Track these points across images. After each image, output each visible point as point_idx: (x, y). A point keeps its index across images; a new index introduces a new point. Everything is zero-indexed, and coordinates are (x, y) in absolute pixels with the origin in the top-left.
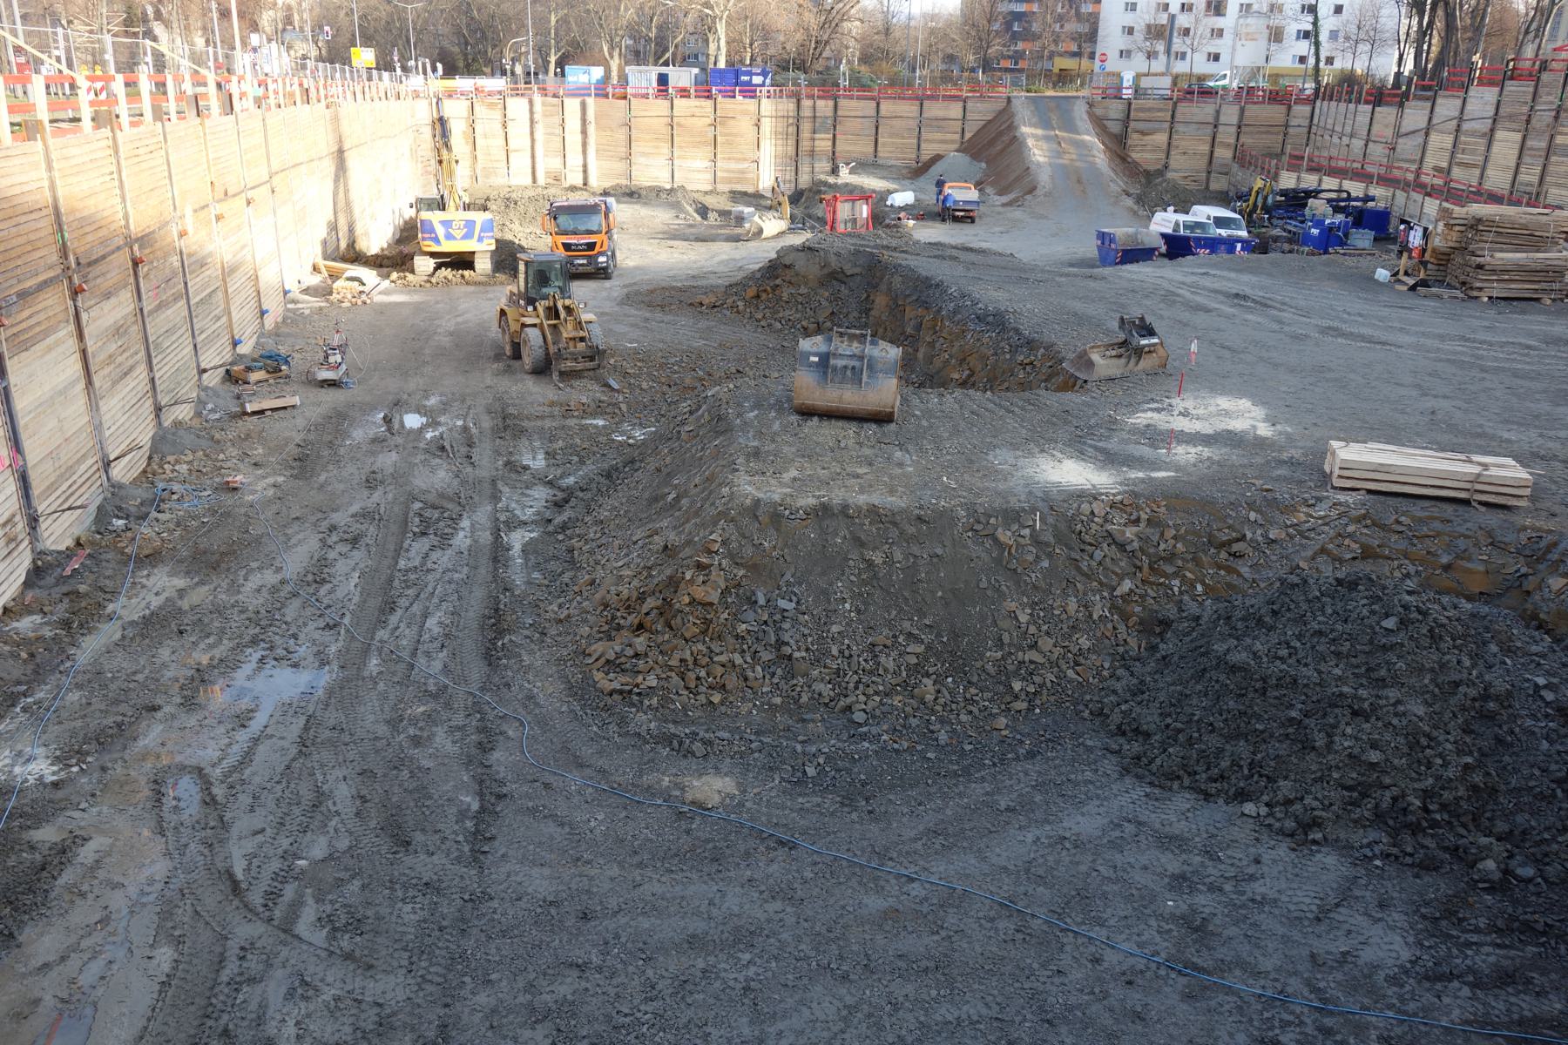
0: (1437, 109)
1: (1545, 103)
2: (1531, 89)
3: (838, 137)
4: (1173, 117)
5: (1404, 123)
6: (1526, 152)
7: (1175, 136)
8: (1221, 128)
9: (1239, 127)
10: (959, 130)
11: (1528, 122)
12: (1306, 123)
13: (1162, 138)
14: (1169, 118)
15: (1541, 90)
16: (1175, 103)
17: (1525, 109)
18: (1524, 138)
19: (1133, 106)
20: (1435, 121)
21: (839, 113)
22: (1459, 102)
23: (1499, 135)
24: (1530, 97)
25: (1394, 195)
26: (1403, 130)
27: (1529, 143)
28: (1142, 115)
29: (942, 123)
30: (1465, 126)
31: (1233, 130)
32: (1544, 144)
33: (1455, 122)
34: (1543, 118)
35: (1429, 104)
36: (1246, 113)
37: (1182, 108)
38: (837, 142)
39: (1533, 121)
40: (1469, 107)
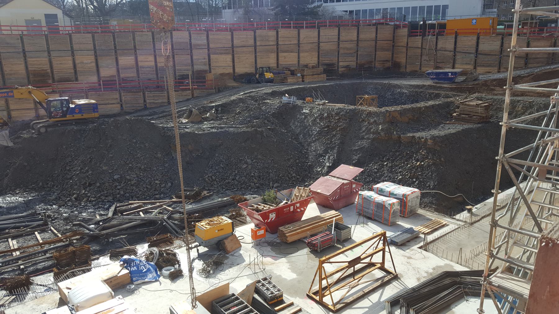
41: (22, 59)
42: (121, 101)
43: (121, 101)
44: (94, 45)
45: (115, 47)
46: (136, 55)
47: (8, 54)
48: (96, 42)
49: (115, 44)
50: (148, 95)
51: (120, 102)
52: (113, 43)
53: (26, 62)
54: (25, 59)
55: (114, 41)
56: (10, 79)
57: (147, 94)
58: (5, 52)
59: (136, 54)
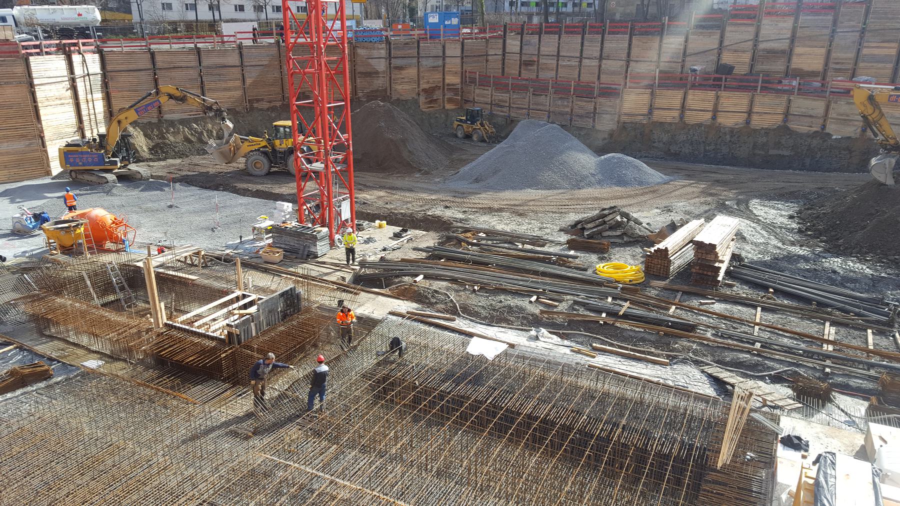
3: (113, 94)
4: (418, 54)
7: (421, 69)
8: (448, 60)
9: (462, 58)
10: (240, 77)
12: (500, 52)
18: (829, 52)
20: (726, 43)
21: (109, 68)
23: (798, 50)
24: (830, 24)
26: (688, 52)
28: (399, 53)
29: (224, 71)
30: (762, 46)
31: (458, 60)
33: (751, 43)
36: (465, 48)
38: (113, 102)
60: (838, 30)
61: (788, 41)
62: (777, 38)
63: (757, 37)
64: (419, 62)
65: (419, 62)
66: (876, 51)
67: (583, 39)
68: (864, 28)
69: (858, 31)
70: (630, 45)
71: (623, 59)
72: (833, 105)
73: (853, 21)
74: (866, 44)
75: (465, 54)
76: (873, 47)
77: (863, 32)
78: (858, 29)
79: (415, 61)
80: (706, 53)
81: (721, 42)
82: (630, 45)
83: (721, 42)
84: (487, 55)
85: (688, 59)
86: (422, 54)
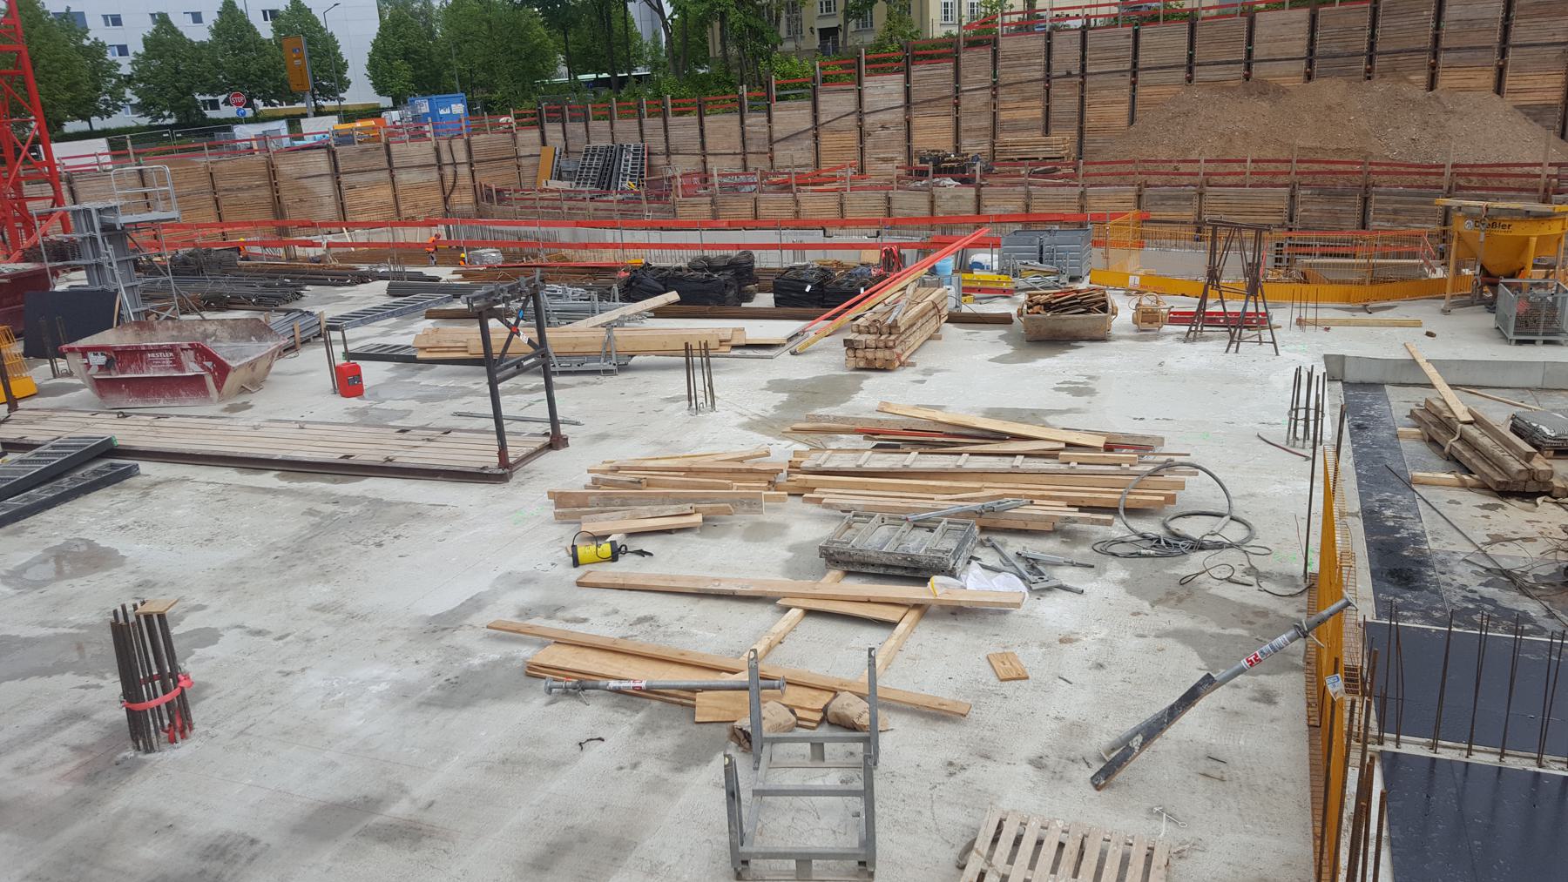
0: (821, 107)
1: (976, 82)
2: (950, 71)
4: (390, 162)
5: (776, 128)
6: (962, 134)
7: (399, 187)
9: (471, 165)
11: (957, 106)
13: (385, 194)
14: (385, 165)
15: (963, 72)
16: (387, 146)
17: (948, 92)
19: (338, 156)
20: (822, 119)
22: (852, 97)
23: (917, 122)
24: (951, 81)
25: (889, 200)
26: (776, 136)
27: (963, 125)
28: (353, 166)
30: (868, 120)
32: (986, 122)
33: (853, 117)
34: (975, 101)
35: (809, 103)
37: (394, 148)
39: (963, 102)
40: (867, 99)
41: (1127, 91)
42: (1291, 220)
43: (1291, 220)
44: (1312, 41)
45: (1372, 46)
46: (1434, 68)
47: (1100, 77)
48: (1318, 35)
49: (1373, 35)
50: (1378, 206)
51: (1287, 222)
52: (1368, 32)
53: (1134, 97)
54: (1134, 90)
55: (1374, 25)
56: (1094, 141)
57: (1377, 201)
58: (1095, 74)
59: (1434, 67)
60: (963, 88)
61: (902, 109)
62: (887, 106)
63: (860, 107)
64: (393, 177)
65: (393, 177)
66: (1018, 114)
67: (641, 124)
68: (995, 83)
69: (988, 88)
70: (702, 131)
71: (697, 152)
72: (938, 202)
73: (979, 73)
74: (1001, 106)
75: (475, 158)
76: (1012, 109)
77: (995, 87)
78: (987, 85)
79: (385, 175)
80: (799, 136)
81: (816, 118)
82: (702, 131)
83: (816, 118)
84: (518, 157)
85: (776, 146)
86: (396, 162)
